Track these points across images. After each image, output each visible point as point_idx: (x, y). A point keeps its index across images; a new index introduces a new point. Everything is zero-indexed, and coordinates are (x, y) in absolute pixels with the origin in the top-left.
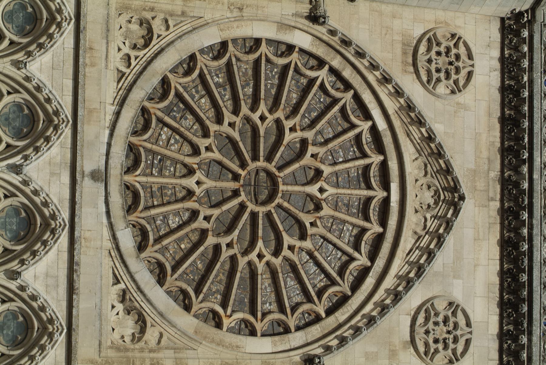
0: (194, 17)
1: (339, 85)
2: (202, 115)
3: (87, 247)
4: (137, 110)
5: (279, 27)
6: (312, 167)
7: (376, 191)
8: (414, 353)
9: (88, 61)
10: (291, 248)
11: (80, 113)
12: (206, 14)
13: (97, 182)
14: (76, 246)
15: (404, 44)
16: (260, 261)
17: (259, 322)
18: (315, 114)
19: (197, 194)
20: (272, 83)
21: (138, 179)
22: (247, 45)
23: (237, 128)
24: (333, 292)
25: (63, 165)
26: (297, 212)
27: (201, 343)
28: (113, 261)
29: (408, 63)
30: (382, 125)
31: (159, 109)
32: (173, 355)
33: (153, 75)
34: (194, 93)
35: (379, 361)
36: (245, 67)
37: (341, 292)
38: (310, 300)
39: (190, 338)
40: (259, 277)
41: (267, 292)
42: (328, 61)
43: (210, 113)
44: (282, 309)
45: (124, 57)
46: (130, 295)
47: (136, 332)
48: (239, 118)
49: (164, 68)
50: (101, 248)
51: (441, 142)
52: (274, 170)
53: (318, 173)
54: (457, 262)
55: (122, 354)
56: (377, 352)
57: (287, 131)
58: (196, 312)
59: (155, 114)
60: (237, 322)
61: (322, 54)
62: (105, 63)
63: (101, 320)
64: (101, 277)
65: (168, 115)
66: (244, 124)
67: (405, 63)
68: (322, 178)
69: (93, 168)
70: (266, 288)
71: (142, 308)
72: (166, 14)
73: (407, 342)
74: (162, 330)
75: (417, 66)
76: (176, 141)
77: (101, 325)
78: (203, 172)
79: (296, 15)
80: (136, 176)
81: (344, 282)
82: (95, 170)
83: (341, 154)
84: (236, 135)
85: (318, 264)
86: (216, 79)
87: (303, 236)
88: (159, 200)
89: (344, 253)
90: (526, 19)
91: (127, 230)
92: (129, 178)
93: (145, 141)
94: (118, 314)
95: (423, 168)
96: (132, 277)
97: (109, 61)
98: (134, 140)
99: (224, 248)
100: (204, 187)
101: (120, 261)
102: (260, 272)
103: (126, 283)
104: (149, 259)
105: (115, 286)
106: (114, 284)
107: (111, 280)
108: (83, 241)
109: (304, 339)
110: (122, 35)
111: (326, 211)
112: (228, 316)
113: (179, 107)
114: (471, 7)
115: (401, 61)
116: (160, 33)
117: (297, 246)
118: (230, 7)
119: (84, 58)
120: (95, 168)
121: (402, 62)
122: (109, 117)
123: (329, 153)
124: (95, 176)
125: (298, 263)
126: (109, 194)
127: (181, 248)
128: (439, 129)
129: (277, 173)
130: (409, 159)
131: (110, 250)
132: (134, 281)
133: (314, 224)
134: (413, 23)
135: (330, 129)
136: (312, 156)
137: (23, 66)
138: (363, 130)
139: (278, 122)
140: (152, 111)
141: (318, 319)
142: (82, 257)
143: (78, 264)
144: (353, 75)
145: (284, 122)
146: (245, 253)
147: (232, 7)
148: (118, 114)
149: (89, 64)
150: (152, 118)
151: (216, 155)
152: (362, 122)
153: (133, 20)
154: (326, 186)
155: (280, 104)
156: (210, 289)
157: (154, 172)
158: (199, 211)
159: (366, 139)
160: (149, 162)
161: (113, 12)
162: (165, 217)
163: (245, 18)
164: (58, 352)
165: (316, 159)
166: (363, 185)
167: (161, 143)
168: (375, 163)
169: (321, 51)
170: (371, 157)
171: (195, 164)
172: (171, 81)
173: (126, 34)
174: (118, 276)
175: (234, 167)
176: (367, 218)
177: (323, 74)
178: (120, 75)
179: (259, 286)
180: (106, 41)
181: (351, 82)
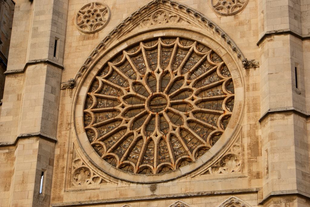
2: (122, 137)
3: (190, 189)
4: (120, 171)
6: (147, 78)
7: (158, 44)
8: (240, 12)
9: (96, 199)
10: (188, 84)
11: (122, 200)
13: (157, 188)
14: (189, 195)
15: (84, 40)
17: (227, 95)
18: (121, 80)
19: (162, 135)
21: (155, 167)
23: (129, 119)
24: (210, 59)
27: (238, 124)
28: (197, 175)
30: (125, 46)
33: (103, 164)
34: (112, 143)
35: (245, 30)
39: (236, 130)
40: (204, 98)
44: (221, 84)
46: (215, 164)
48: (124, 118)
49: (98, 159)
50: (190, 182)
51: (132, 14)
55: (245, 165)
56: (240, 32)
57: (129, 93)
58: (223, 129)
59: (122, 162)
60: (228, 107)
64: (205, 180)
65: (123, 155)
66: (127, 116)
68: (152, 72)
70: (210, 94)
71: (221, 157)
73: (234, 17)
74: (232, 145)
75: (94, 31)
76: (137, 149)
77: (230, 178)
79: (71, 96)
80: (154, 167)
81: (205, 54)
85: (196, 69)
88: (166, 154)
92: (154, 172)
95: (146, 21)
96: (205, 164)
98: (135, 171)
101: (197, 171)
102: (201, 98)
103: (208, 167)
105: (210, 173)
108: (187, 192)
109: (235, 71)
111: (169, 68)
112: (224, 112)
113: (119, 150)
114: (64, 8)
115: (92, 40)
117: (187, 81)
119: (94, 201)
120: (150, 189)
122: (124, 184)
123: (140, 71)
124: (153, 189)
125: (196, 79)
127: (190, 141)
128: (125, 16)
130: (141, 29)
132: (207, 163)
135: (128, 72)
139: (125, 99)
140: (121, 163)
142: (195, 191)
143: (199, 193)
145: (125, 95)
147: (68, 128)
148: (122, 180)
149: (97, 198)
150: (124, 163)
154: (157, 70)
155: (116, 98)
156: (211, 123)
157: (152, 159)
160: (147, 162)
162: (175, 151)
165: (143, 77)
166: (155, 51)
167: (137, 157)
168: (144, 46)
169: (89, 81)
171: (147, 138)
172: (106, 155)
174: (205, 171)
175: (148, 118)
179: (208, 98)
181: (104, 64)
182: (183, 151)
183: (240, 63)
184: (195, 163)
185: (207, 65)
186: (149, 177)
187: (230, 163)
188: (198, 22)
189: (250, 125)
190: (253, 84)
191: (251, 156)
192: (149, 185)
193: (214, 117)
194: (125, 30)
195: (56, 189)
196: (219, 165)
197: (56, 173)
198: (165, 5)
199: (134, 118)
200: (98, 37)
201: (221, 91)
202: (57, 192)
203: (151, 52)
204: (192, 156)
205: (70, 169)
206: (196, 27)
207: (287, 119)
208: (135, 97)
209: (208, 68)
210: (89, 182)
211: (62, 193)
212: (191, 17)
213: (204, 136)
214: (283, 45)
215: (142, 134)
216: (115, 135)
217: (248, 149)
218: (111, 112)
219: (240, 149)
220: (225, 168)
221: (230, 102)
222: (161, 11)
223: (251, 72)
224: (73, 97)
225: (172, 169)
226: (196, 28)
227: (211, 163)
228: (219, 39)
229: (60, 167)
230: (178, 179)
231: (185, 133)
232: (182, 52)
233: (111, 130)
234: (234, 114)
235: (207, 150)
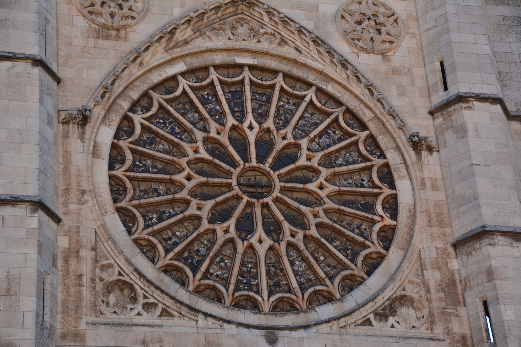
0: (96, 239)
2: (194, 235)
5: (96, 156)
12: (92, 227)
13: (278, 337)
15: (98, 37)
17: (383, 190)
20: (152, 167)
28: (349, 324)
29: (117, 36)
30: (180, 67)
31: (194, 276)
32: (429, 271)
33: (162, 280)
34: (172, 242)
35: (405, 84)
36: (138, 192)
37: (343, 115)
40: (342, 188)
41: (352, 182)
42: (124, 111)
43: (189, 228)
45: (146, 309)
46: (379, 309)
47: (412, 306)
48: (192, 199)
49: (152, 269)
52: (239, 170)
54: (303, 8)
55: (437, 319)
56: (397, 86)
57: (198, 156)
59: (200, 280)
61: (118, 117)
62: (156, 328)
63: (409, 338)
67: (117, 38)
69: (265, 342)
70: (349, 183)
71: (389, 298)
72: (96, 267)
74: (407, 280)
77: (413, 338)
78: (249, 236)
80: (263, 300)
82: (266, 340)
86: (155, 220)
91: (317, 310)
94: (398, 322)
97: (153, 324)
98: (228, 301)
99: (318, 220)
100: (264, 236)
102: (336, 188)
104: (340, 290)
106: (371, 324)
107: (368, 327)
109: (392, 150)
110: (122, 311)
115: (116, 42)
116: (117, 273)
118: (83, 202)
121: (116, 40)
125: (323, 153)
126: (287, 326)
129: (242, 167)
131: (340, 328)
133: (283, 136)
134: (74, 26)
135: (189, 116)
136: (218, 133)
138: (187, 84)
140: (197, 283)
144: (135, 89)
148: (206, 315)
149: (160, 344)
152: (179, 85)
153: (105, 299)
157: (255, 283)
158: (288, 241)
159: (195, 82)
160: (246, 288)
161: (100, 320)
162: (298, 275)
168: (218, 75)
170: (213, 80)
173: (120, 307)
174: (363, 320)
178: (165, 314)
179: (350, 189)
180: (134, 327)
183: (402, 139)
184: (342, 302)
185: (337, 132)
186: (257, 315)
187: (403, 311)
188: (317, 54)
189: (436, 248)
190: (432, 178)
191: (446, 303)
192: (263, 332)
193: (361, 225)
194: (179, 36)
195: (68, 316)
196: (387, 312)
197: (65, 285)
198: (253, 9)
200: (128, 39)
201: (369, 181)
202: (70, 323)
203: (231, 89)
204: (334, 288)
206: (314, 61)
207: (518, 247)
209: (340, 137)
210: (135, 312)
211: (82, 326)
212: (303, 41)
214: (491, 120)
215: (233, 233)
216: (176, 228)
217: (438, 291)
218: (164, 184)
220: (396, 318)
222: (244, 19)
223: (425, 158)
224: (87, 141)
225: (298, 306)
226: (313, 62)
227: (372, 306)
228: (360, 90)
229: (72, 274)
230: (316, 328)
231: (312, 245)
232: (288, 100)
233: (169, 217)
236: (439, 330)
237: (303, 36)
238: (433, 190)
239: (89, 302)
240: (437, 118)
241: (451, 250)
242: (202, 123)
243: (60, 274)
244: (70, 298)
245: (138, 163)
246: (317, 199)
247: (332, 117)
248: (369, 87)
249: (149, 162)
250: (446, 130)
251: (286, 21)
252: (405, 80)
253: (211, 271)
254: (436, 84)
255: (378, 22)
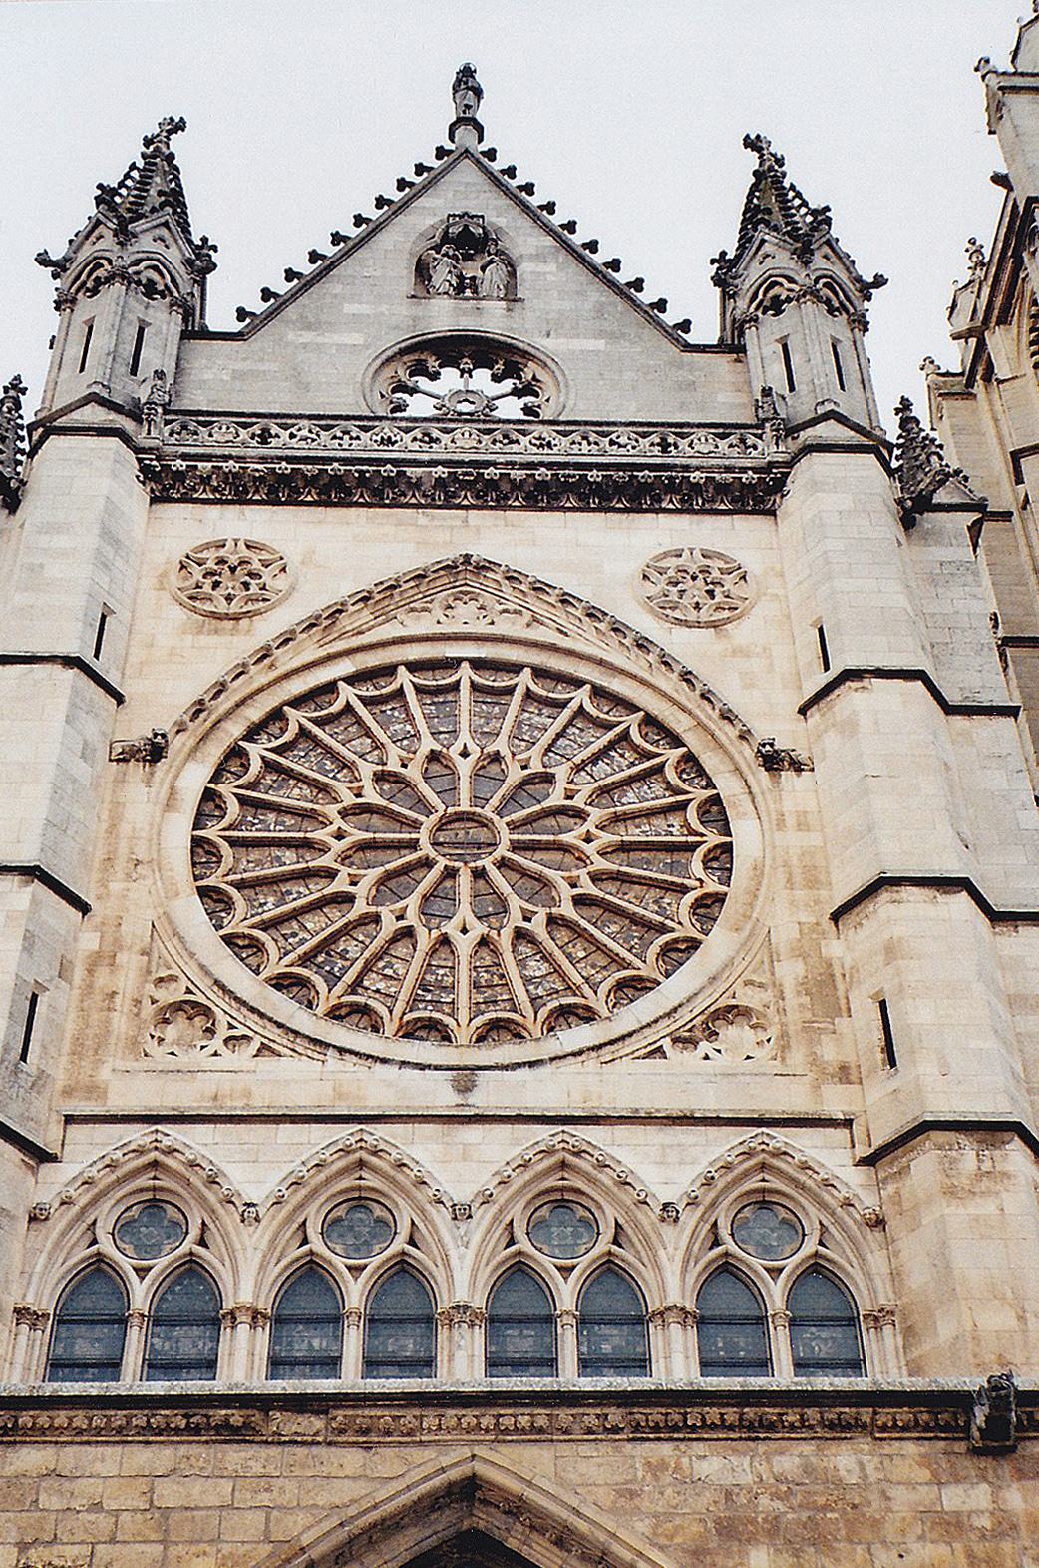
1: (274, 728)
9: (240, 1103)
15: (200, 632)
16: (598, 838)
17: (705, 839)
21: (463, 1021)
22: (204, 860)
25: (445, 1139)
26: (505, 786)
30: (346, 667)
34: (297, 940)
37: (639, 725)
38: (659, 769)
40: (625, 839)
45: (231, 1047)
52: (434, 818)
53: (434, 756)
55: (793, 1042)
68: (444, 750)
70: (643, 832)
72: (146, 981)
76: (389, 965)
79: (148, 783)
80: (458, 1024)
81: (621, 722)
83: (397, 726)
84: (375, 873)
85: (595, 759)
87: (549, 778)
89: (570, 723)
90: (154, 463)
93: (391, 1012)
94: (719, 1051)
98: (390, 1028)
104: (611, 1005)
107: (657, 1062)
109: (727, 774)
111: (500, 745)
124: (464, 1088)
127: (585, 957)
137: (252, 1209)
141: (690, 758)
146: (583, 860)
147: (134, 876)
148: (342, 1050)
151: (412, 902)
153: (157, 1034)
154: (458, 746)
157: (450, 1000)
160: (430, 1008)
163: (155, 857)
164: (808, 1143)
166: (450, 697)
167: (393, 990)
169: (215, 751)
176: (509, 691)
177: (256, 751)
182: (560, 986)
183: (746, 753)
194: (345, 622)
195: (80, 1059)
196: (698, 1033)
199: (381, 870)
202: (81, 1071)
203: (436, 699)
205: (137, 1002)
207: (947, 904)
208: (382, 814)
211: (104, 1074)
213: (633, 947)
215: (412, 919)
219: (768, 996)
221: (721, 858)
229: (97, 992)
234: (737, 890)
235: (646, 988)
236: (797, 1058)
237: (571, 609)
238: (800, 830)
239: (123, 1037)
240: (812, 715)
241: (828, 926)
242: (376, 752)
243: (76, 992)
244: (87, 1031)
245: (250, 819)
246: (579, 859)
247: (618, 729)
248: (687, 677)
249: (271, 816)
250: (826, 731)
251: (540, 588)
252: (756, 664)
253: (366, 983)
254: (810, 664)
255: (709, 580)
